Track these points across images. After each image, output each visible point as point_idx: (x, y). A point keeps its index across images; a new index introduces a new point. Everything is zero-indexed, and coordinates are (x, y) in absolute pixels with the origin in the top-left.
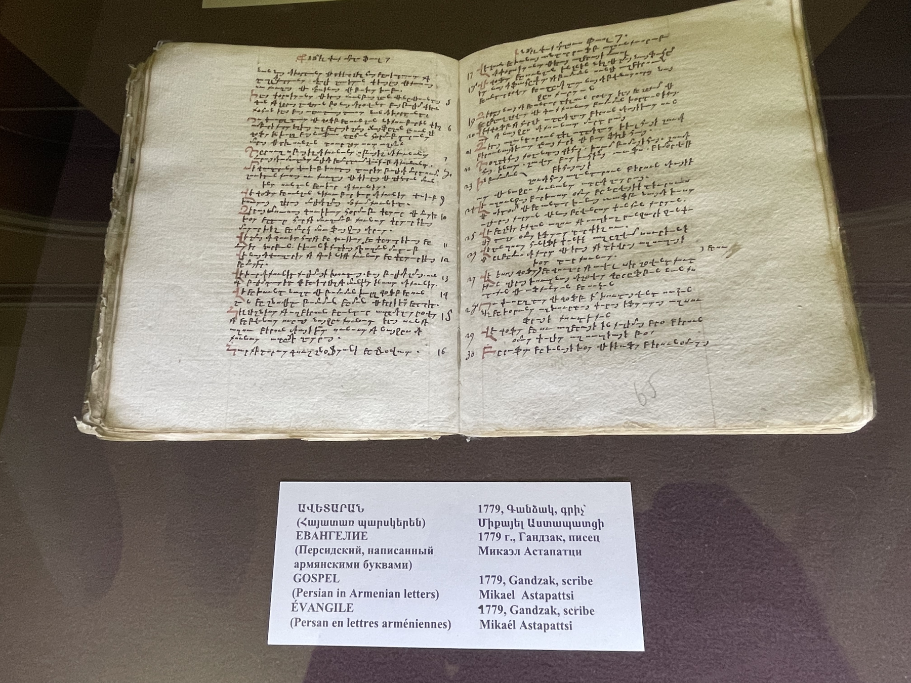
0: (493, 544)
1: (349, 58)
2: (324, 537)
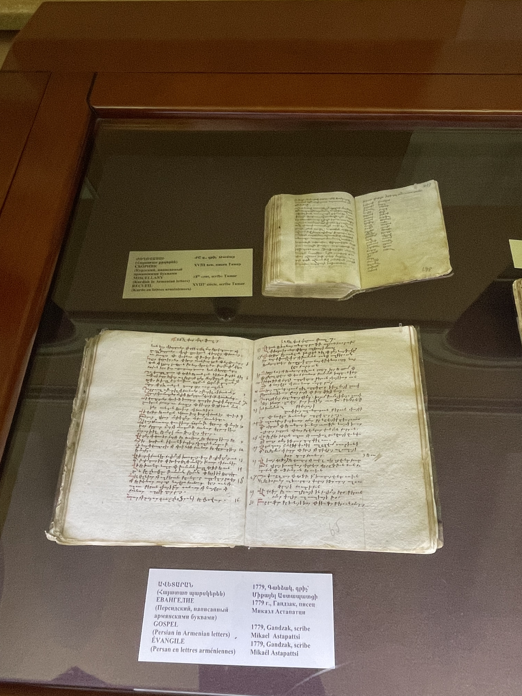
0: (259, 607)
1: (198, 340)
2: (171, 601)
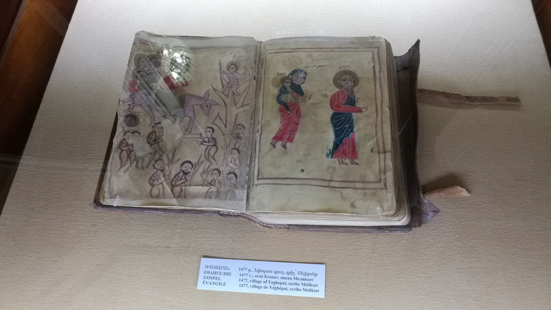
2: (215, 274)
